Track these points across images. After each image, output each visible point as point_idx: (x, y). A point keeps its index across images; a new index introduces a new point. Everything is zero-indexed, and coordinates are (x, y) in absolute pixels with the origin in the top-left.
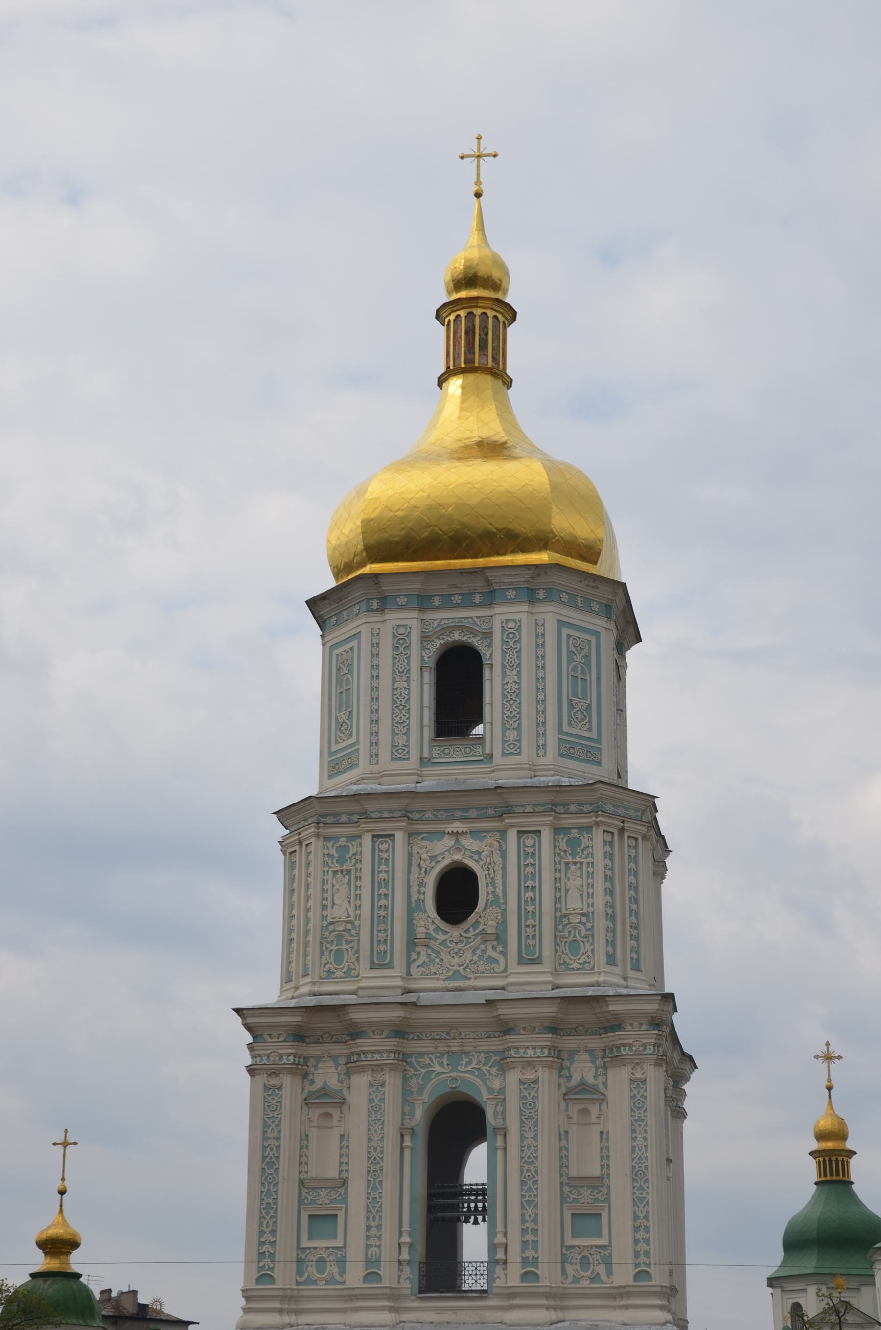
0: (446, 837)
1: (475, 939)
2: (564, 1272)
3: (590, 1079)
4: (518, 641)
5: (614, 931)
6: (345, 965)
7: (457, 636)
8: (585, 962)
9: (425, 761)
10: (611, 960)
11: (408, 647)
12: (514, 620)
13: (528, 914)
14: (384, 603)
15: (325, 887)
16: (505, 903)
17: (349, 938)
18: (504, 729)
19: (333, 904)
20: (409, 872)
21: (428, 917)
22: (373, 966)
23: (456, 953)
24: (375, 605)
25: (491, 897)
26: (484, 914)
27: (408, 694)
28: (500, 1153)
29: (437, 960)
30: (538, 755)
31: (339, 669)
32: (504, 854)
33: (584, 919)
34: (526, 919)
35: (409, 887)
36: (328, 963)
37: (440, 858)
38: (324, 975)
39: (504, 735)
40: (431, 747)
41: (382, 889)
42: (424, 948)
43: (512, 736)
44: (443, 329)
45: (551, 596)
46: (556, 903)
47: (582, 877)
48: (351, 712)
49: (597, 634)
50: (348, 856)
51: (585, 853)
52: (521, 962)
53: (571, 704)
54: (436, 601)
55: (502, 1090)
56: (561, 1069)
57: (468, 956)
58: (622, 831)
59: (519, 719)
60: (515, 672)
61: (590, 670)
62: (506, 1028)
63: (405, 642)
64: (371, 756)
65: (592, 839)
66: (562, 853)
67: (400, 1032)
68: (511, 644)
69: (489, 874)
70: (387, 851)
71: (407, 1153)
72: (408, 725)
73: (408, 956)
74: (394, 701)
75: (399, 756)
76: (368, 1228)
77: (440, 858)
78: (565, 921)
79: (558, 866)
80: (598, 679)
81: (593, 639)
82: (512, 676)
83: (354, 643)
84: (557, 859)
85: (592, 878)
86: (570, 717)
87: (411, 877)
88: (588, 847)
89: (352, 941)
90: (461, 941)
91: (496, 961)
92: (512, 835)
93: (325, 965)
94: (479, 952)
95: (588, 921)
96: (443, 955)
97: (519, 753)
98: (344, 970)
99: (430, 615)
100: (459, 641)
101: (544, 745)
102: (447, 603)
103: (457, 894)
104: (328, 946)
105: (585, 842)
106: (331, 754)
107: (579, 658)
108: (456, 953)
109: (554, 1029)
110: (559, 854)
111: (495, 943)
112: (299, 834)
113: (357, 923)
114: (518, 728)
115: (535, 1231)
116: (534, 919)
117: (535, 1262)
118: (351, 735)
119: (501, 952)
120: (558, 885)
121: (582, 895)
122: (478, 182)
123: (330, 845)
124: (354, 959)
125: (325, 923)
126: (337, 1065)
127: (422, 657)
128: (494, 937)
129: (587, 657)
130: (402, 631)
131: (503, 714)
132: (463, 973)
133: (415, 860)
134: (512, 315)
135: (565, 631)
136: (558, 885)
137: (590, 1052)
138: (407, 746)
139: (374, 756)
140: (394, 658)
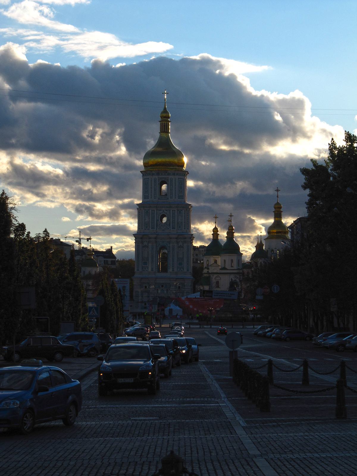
2: (177, 270)
3: (181, 245)
7: (163, 180)
10: (185, 229)
14: (153, 175)
18: (170, 195)
28: (169, 255)
31: (145, 183)
32: (170, 213)
43: (171, 195)
45: (177, 174)
49: (183, 179)
53: (180, 191)
54: (160, 174)
55: (170, 246)
62: (171, 238)
73: (157, 227)
81: (183, 180)
83: (148, 179)
99: (159, 176)
106: (144, 195)
107: (181, 183)
114: (172, 195)
117: (174, 269)
126: (147, 242)
135: (179, 179)
137: (182, 241)
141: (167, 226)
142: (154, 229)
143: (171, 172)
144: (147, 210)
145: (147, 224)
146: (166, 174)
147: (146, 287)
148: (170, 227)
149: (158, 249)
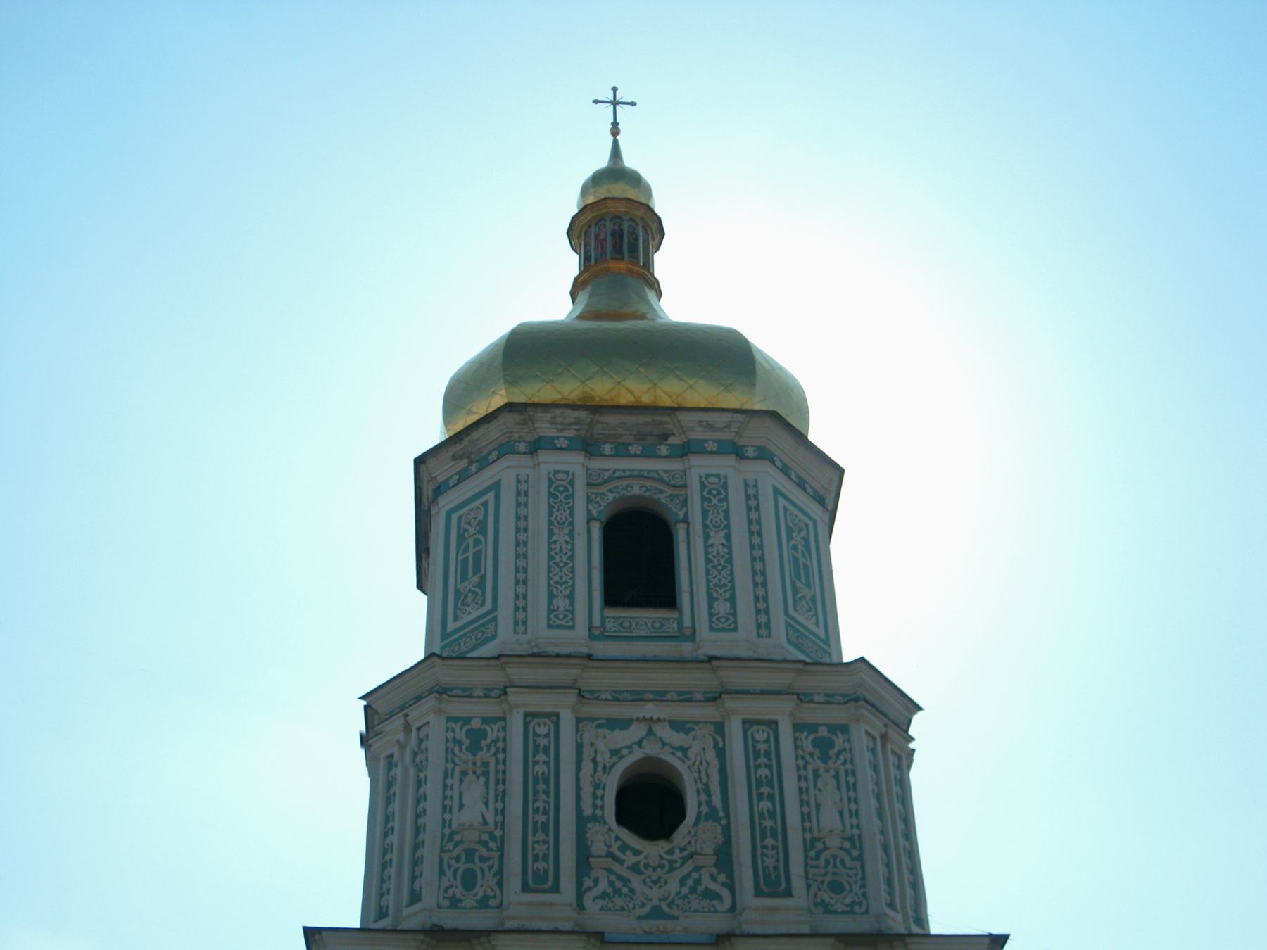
0: (634, 726)
1: (683, 864)
4: (726, 499)
5: (888, 865)
6: (479, 891)
7: (636, 491)
8: (853, 903)
9: (596, 633)
11: (572, 496)
12: (718, 476)
13: (769, 830)
14: (536, 447)
15: (449, 782)
16: (727, 816)
17: (484, 852)
18: (711, 600)
19: (461, 806)
20: (578, 769)
21: (610, 829)
22: (525, 888)
23: (655, 882)
24: (522, 447)
25: (705, 809)
27: (572, 550)
29: (625, 890)
30: (759, 635)
32: (721, 754)
33: (847, 845)
34: (763, 837)
35: (578, 788)
36: (452, 886)
37: (625, 752)
38: (447, 903)
39: (710, 606)
40: (603, 619)
41: (542, 784)
42: (605, 873)
43: (722, 607)
45: (764, 454)
46: (803, 821)
47: (839, 788)
48: (483, 578)
50: (483, 743)
51: (842, 758)
52: (758, 893)
53: (795, 591)
54: (607, 449)
57: (673, 886)
59: (733, 588)
60: (722, 534)
61: (810, 554)
63: (566, 489)
64: (516, 623)
65: (849, 741)
66: (807, 757)
68: (715, 501)
69: (700, 779)
70: (547, 736)
72: (573, 586)
73: (579, 884)
74: (551, 558)
75: (559, 622)
77: (625, 752)
78: (819, 845)
79: (802, 772)
82: (717, 538)
83: (490, 497)
84: (801, 762)
85: (855, 790)
86: (795, 601)
87: (581, 774)
88: (845, 750)
89: (488, 859)
90: (662, 867)
91: (718, 897)
92: (735, 729)
93: (446, 891)
94: (690, 882)
95: (854, 846)
96: (636, 882)
97: (735, 629)
98: (478, 897)
99: (597, 464)
100: (639, 497)
101: (768, 626)
102: (621, 451)
103: (650, 803)
104: (453, 862)
105: (839, 741)
106: (445, 635)
108: (655, 882)
110: (803, 757)
111: (715, 871)
112: (406, 715)
113: (498, 833)
114: (732, 600)
116: (774, 835)
118: (483, 604)
119: (724, 884)
120: (805, 797)
121: (841, 813)
122: (615, 125)
123: (457, 727)
124: (493, 882)
125: (447, 831)
127: (589, 511)
128: (712, 860)
129: (806, 539)
130: (562, 476)
131: (708, 581)
132: (666, 909)
133: (587, 753)
135: (782, 502)
136: (805, 797)
138: (572, 612)
139: (520, 624)
140: (551, 507)
141: (697, 869)
142: (555, 889)
143: (710, 426)
144: (476, 724)
145: (470, 854)
146: (663, 450)
148: (731, 887)
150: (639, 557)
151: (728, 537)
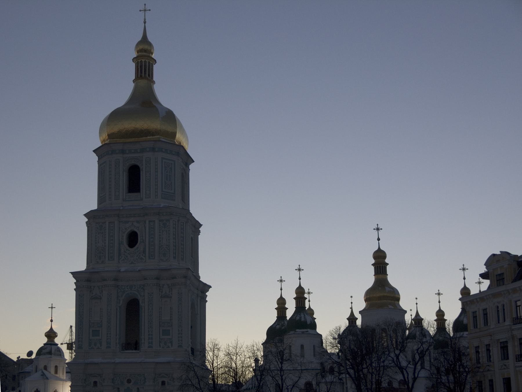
2: (160, 345)
7: (133, 162)
10: (174, 258)
26: (139, 246)
28: (143, 314)
44: (134, 64)
55: (144, 296)
56: (160, 289)
58: (179, 221)
67: (116, 280)
71: (118, 313)
76: (107, 334)
80: (175, 174)
92: (147, 222)
103: (133, 239)
109: (158, 279)
115: (152, 335)
122: (145, 19)
134: (155, 61)
135: (164, 161)
147: (95, 383)
149: (121, 302)
150: (134, 179)
151: (150, 174)
